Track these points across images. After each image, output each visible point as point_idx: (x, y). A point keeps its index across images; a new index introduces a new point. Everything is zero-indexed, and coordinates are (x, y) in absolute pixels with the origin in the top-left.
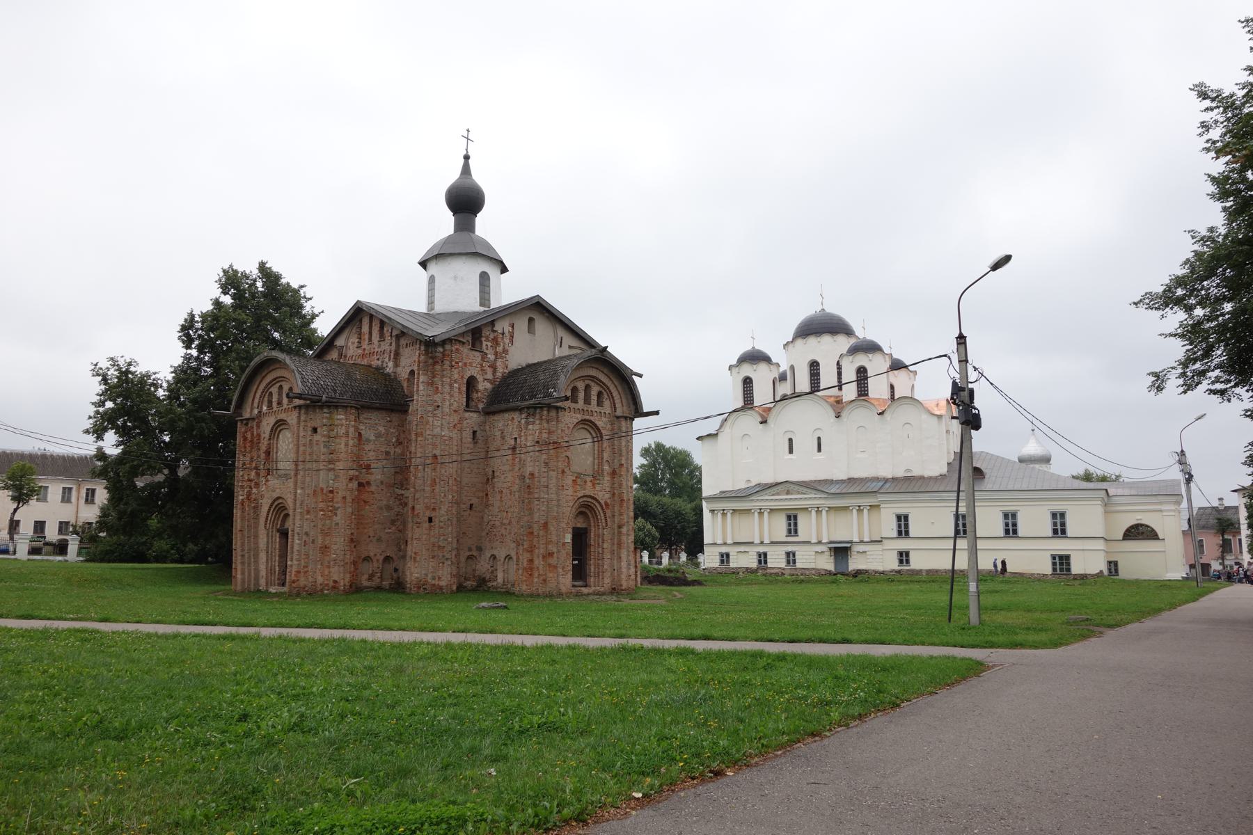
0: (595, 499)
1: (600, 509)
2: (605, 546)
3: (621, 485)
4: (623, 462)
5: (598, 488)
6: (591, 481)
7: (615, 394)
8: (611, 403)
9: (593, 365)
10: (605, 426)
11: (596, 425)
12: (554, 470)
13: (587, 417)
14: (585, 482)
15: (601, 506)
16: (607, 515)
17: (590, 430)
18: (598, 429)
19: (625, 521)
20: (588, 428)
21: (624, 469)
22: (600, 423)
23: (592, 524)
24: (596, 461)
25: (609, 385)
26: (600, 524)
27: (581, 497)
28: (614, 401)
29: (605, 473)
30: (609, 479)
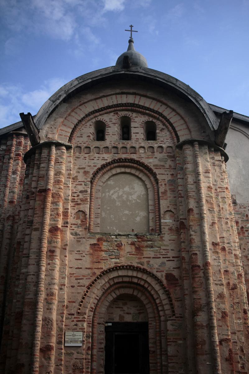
0: (144, 271)
1: (157, 287)
2: (171, 350)
3: (191, 241)
4: (191, 206)
5: (148, 253)
6: (133, 244)
7: (174, 119)
8: (171, 133)
9: (124, 91)
10: (162, 163)
11: (142, 164)
12: (36, 229)
13: (124, 156)
14: (119, 246)
15: (159, 282)
16: (171, 296)
17: (137, 173)
18: (150, 170)
19: (203, 302)
20: (133, 171)
21: (194, 217)
22: (151, 160)
23: (151, 315)
24: (151, 216)
25: (160, 111)
26: (161, 313)
27: (110, 270)
28: (174, 128)
29: (165, 230)
30: (174, 237)
